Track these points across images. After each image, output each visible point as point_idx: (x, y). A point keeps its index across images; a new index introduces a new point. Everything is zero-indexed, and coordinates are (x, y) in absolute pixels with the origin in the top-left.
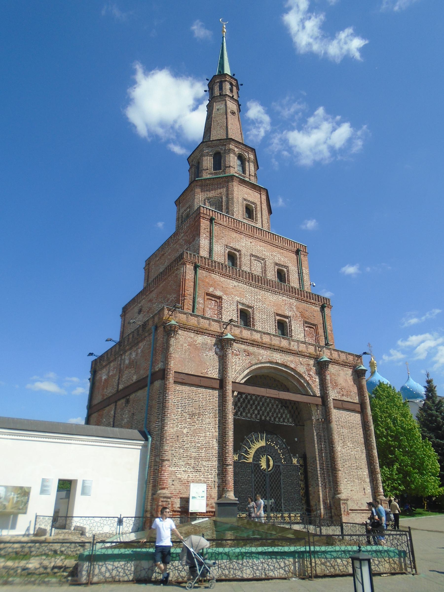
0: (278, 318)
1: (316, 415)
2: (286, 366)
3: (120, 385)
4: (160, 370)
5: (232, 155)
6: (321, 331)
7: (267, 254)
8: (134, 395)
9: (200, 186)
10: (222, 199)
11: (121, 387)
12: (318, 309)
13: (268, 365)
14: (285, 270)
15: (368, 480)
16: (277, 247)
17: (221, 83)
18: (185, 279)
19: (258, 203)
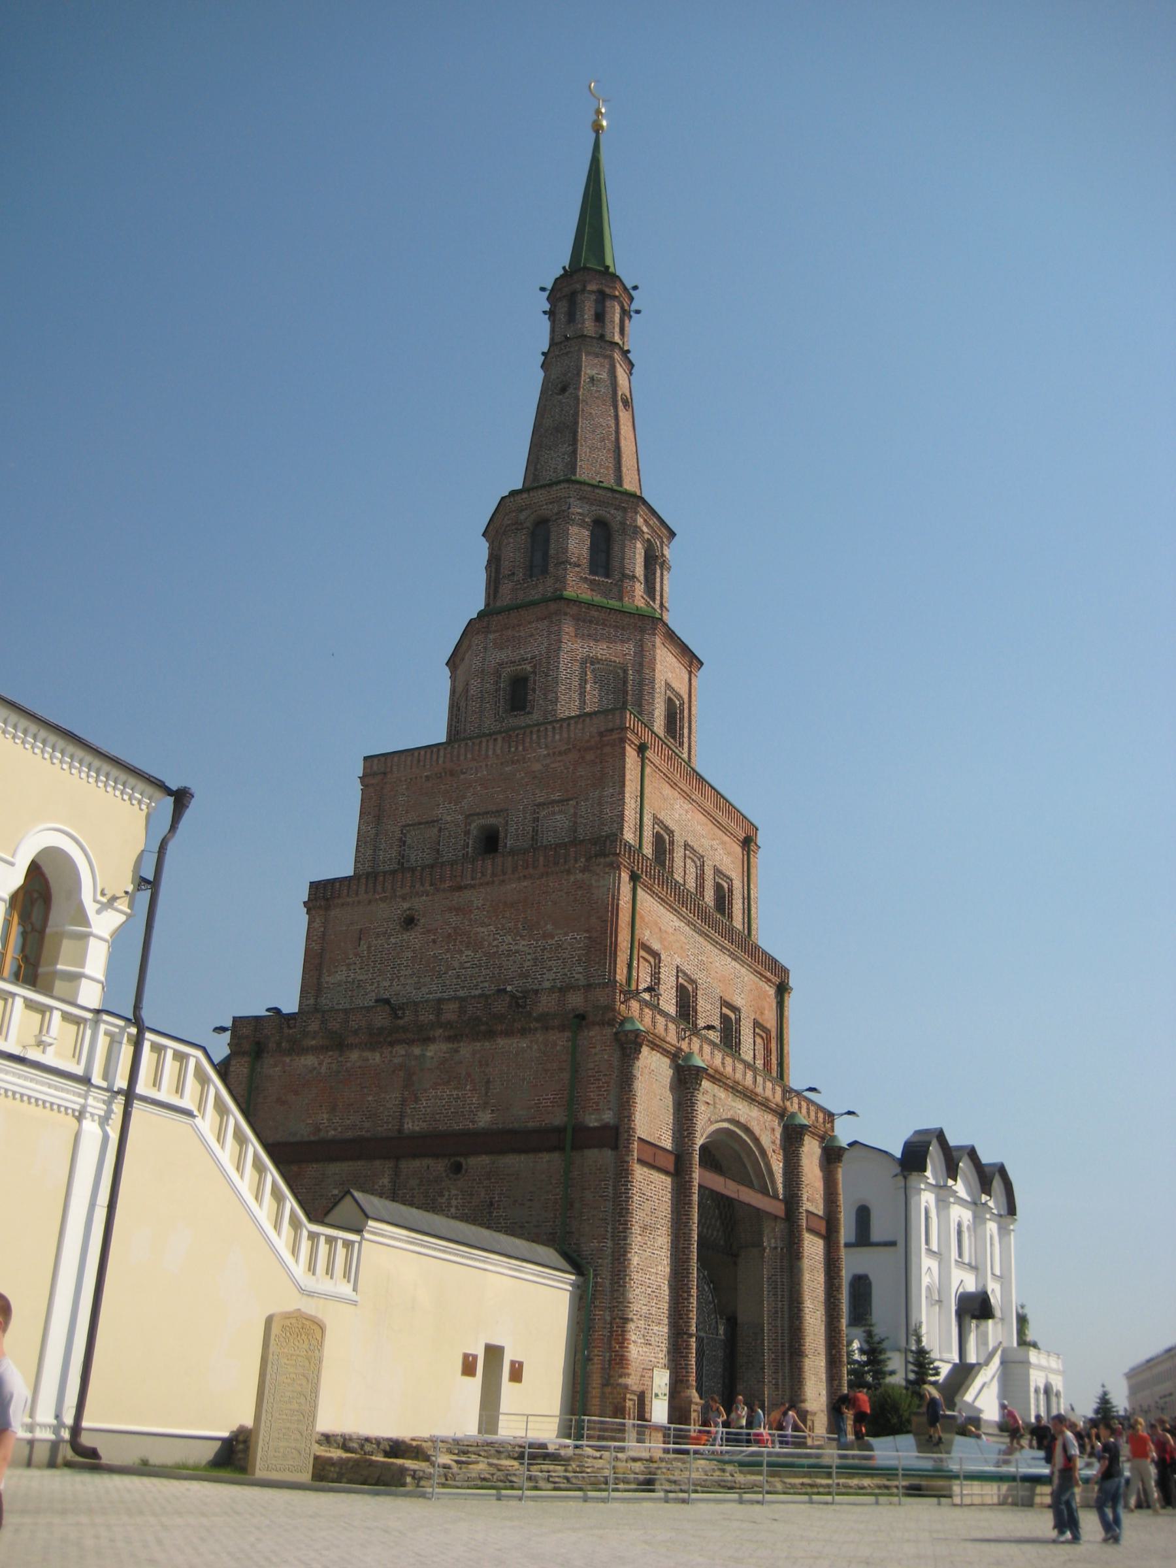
0: (725, 1010)
1: (771, 1240)
2: (747, 1130)
3: (406, 1120)
4: (605, 1127)
5: (639, 545)
6: (773, 1046)
7: (706, 842)
8: (485, 1160)
9: (573, 616)
10: (625, 672)
11: (409, 1126)
12: (771, 991)
13: (725, 1125)
14: (726, 886)
15: (824, 1377)
16: (720, 826)
17: (602, 297)
18: (618, 905)
19: (686, 700)
